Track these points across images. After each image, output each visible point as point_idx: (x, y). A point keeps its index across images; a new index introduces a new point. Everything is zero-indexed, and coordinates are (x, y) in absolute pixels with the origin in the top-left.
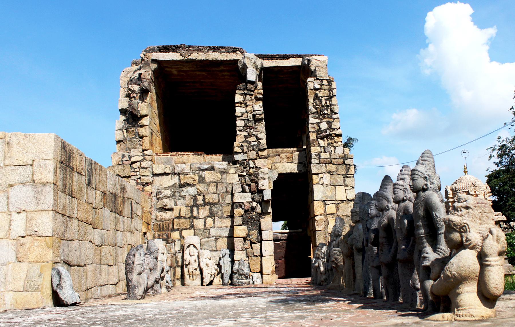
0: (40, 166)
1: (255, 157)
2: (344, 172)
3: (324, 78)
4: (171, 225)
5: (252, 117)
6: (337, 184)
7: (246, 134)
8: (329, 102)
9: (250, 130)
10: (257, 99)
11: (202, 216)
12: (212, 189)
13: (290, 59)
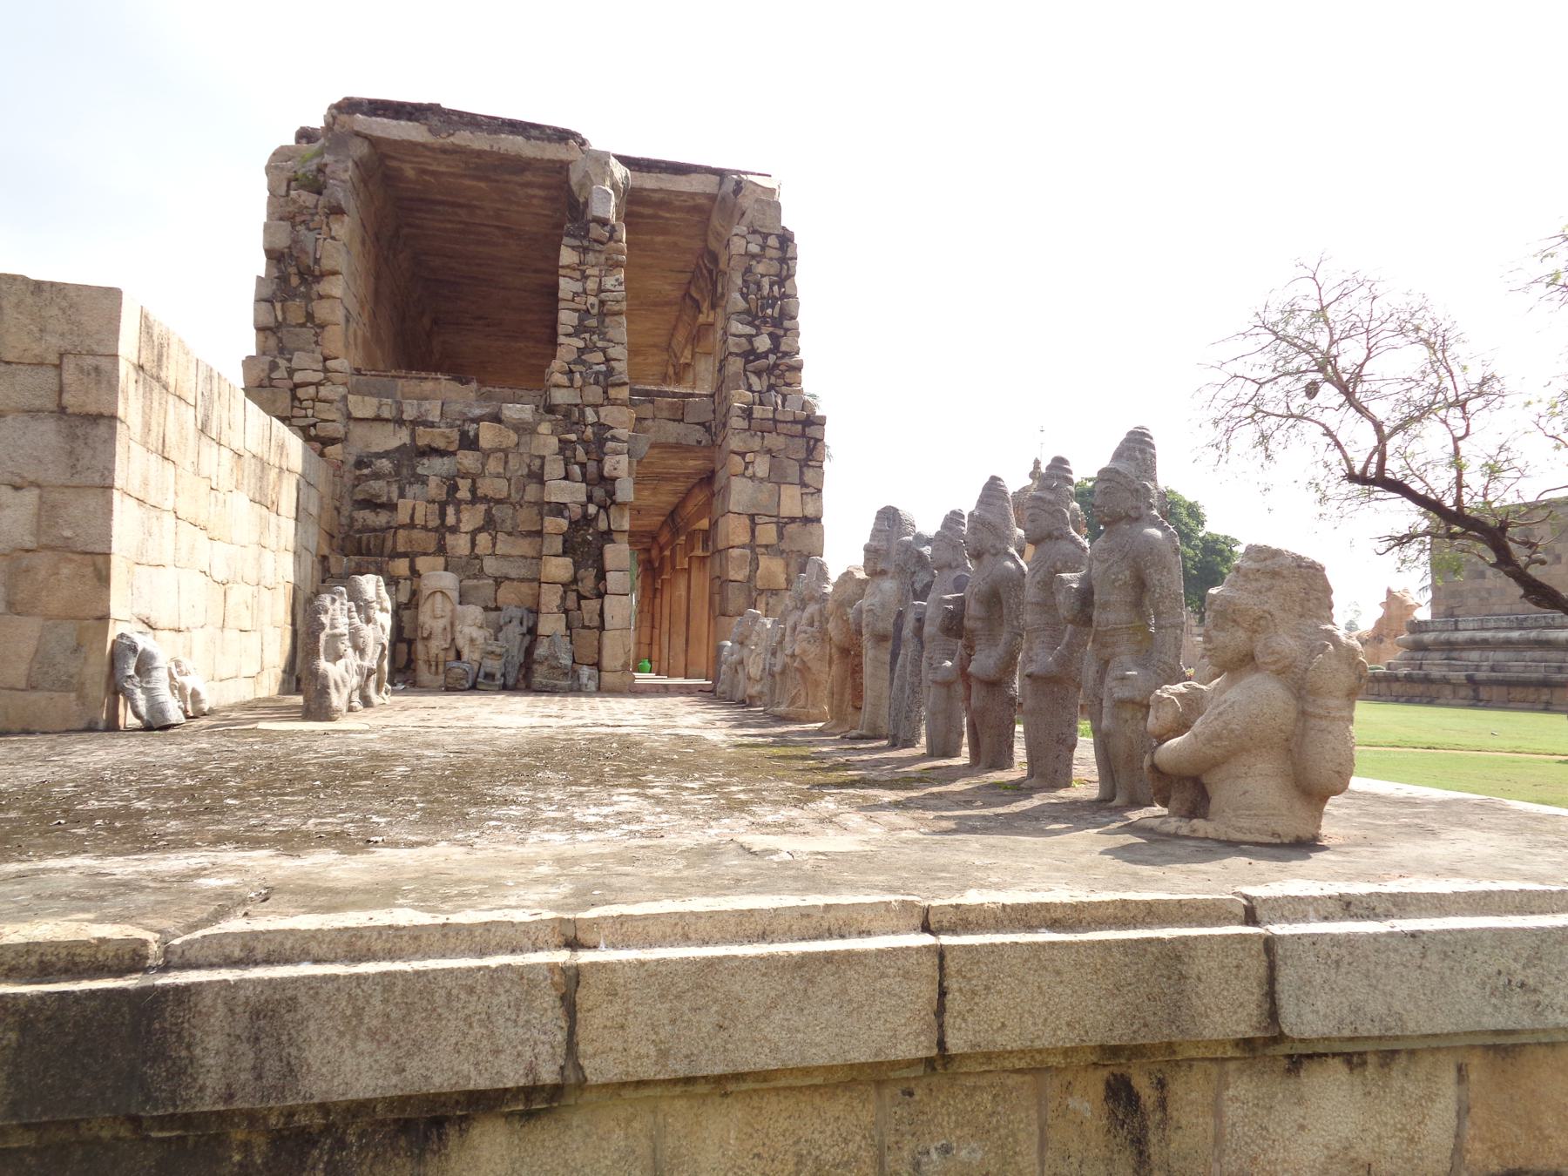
0: (82, 370)
2: (802, 455)
4: (389, 544)
5: (596, 307)
7: (581, 344)
11: (466, 526)
12: (493, 465)
13: (693, 176)
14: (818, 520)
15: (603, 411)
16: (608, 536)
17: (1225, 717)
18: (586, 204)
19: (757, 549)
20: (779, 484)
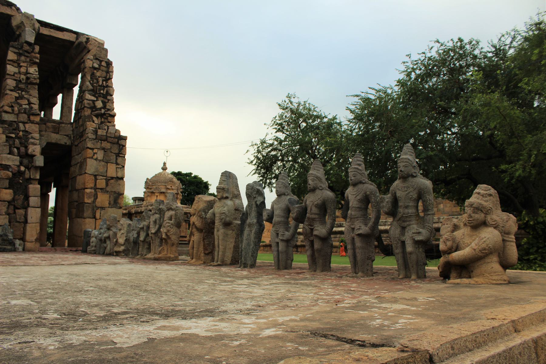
1: (26, 121)
7: (17, 95)
8: (106, 83)
9: (22, 92)
10: (33, 63)
13: (65, 32)
14: (122, 178)
15: (27, 126)
16: (29, 180)
17: (488, 242)
18: (20, 35)
19: (97, 190)
20: (107, 163)
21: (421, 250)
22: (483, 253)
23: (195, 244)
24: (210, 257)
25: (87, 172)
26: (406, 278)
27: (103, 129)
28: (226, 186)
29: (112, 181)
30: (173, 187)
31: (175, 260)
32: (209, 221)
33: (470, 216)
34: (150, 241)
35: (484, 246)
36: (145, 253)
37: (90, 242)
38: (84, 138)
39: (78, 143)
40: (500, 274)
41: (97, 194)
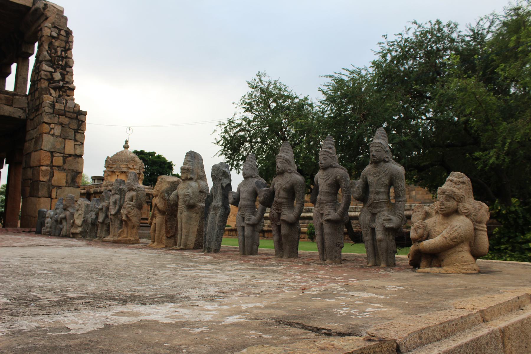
2: (76, 127)
3: (62, 28)
6: (67, 138)
8: (65, 54)
14: (81, 156)
17: (458, 231)
19: (53, 168)
20: (65, 139)
21: (391, 238)
22: (454, 241)
23: (157, 226)
24: (172, 241)
25: (42, 148)
26: (375, 266)
27: (61, 103)
28: (191, 167)
29: (70, 159)
30: (135, 167)
31: (136, 244)
32: (172, 203)
33: (442, 204)
34: (109, 223)
35: (455, 234)
36: (103, 236)
37: (44, 222)
38: (40, 112)
39: (34, 117)
40: (470, 263)
41: (53, 172)
